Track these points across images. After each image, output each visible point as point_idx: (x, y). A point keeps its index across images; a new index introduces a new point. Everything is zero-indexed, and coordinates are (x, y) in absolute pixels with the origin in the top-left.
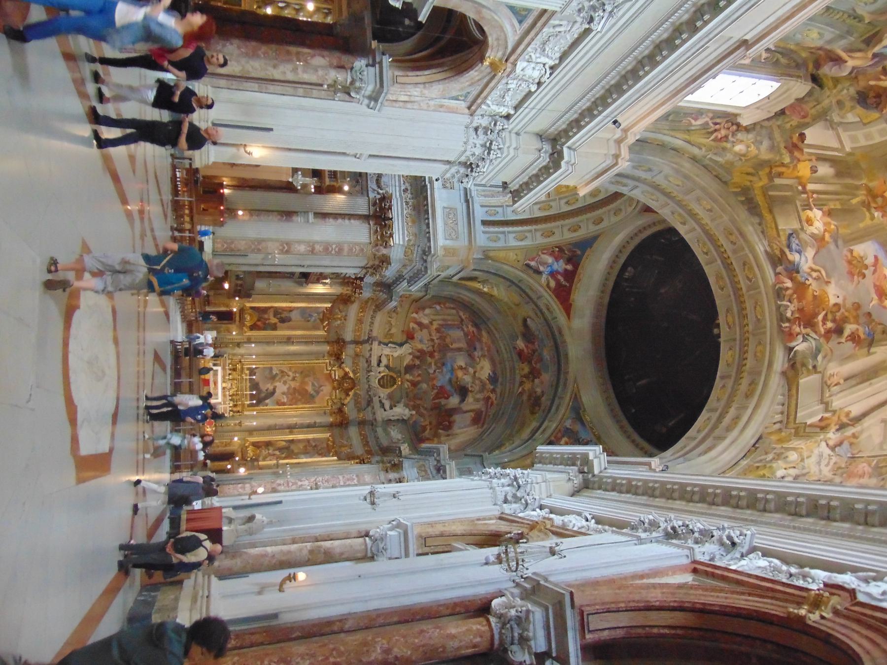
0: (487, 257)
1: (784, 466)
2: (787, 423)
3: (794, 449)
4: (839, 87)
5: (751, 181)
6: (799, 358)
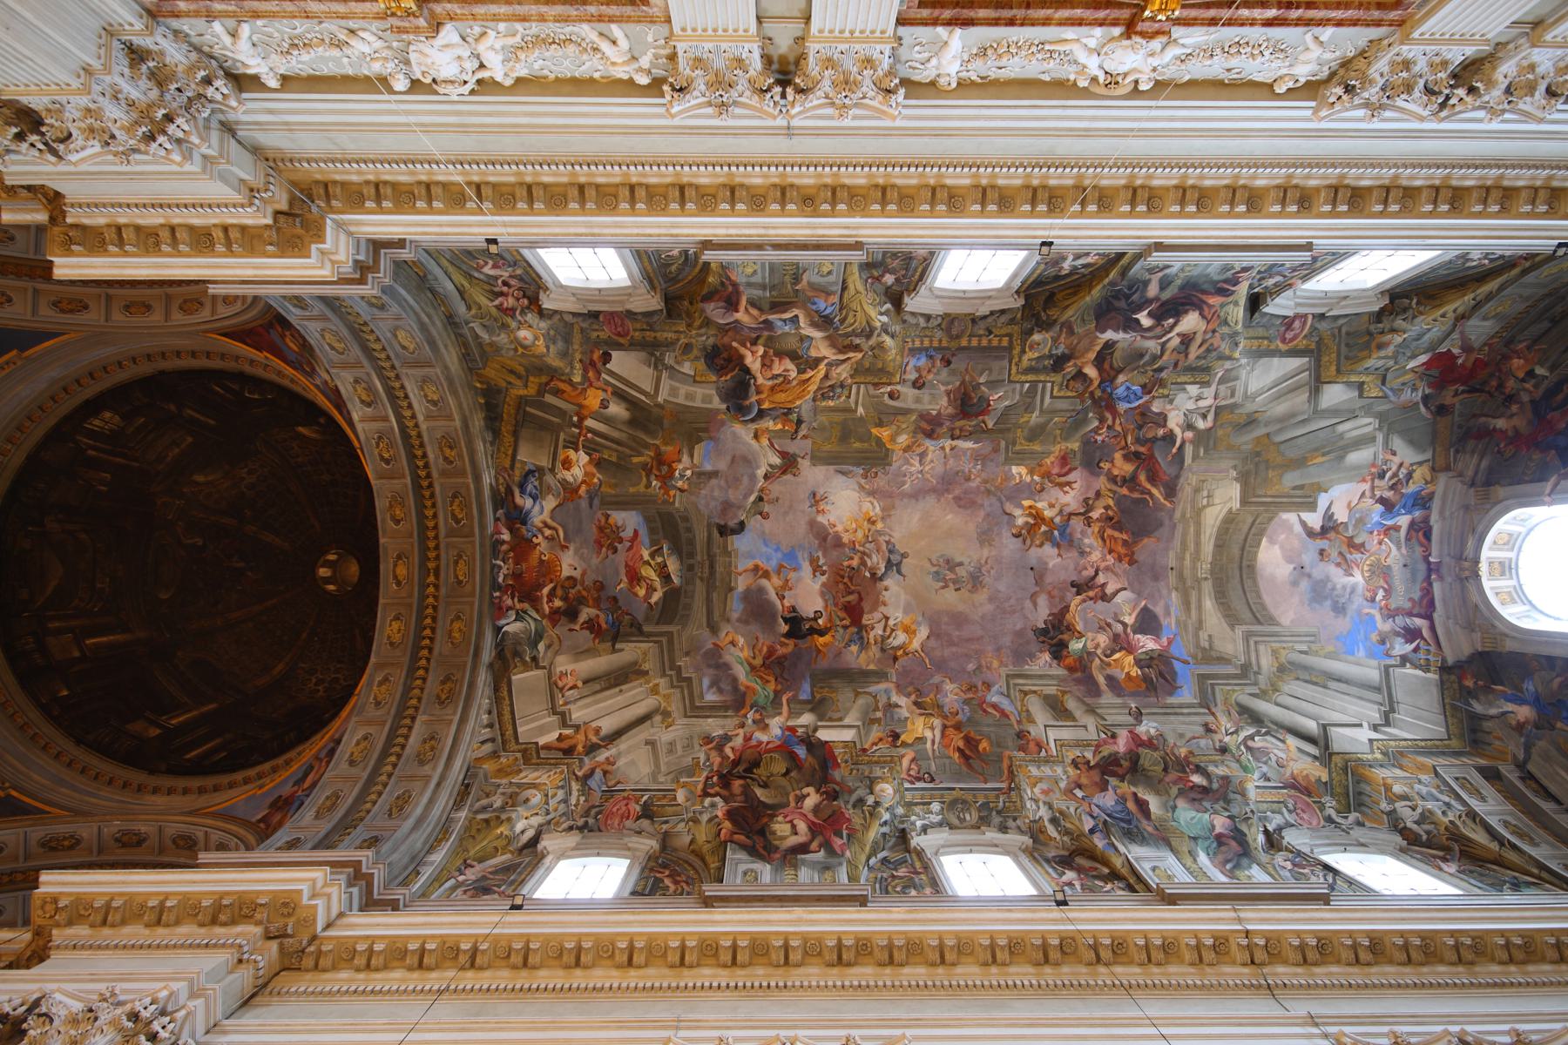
1: (525, 815)
2: (504, 742)
3: (534, 786)
4: (703, 331)
5: (510, 383)
6: (508, 642)
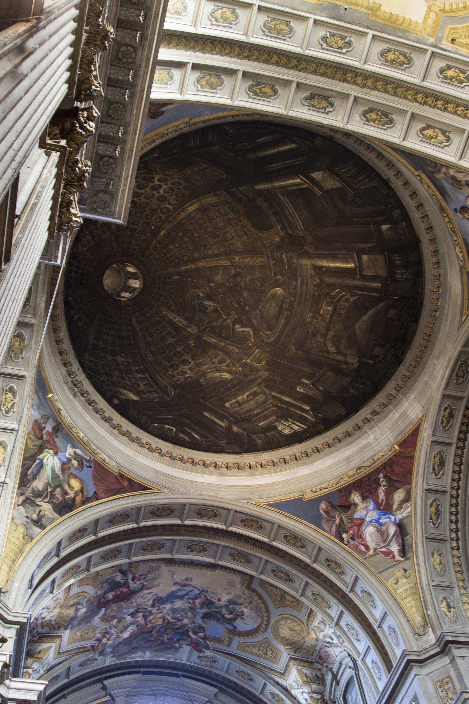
0: (426, 622)
